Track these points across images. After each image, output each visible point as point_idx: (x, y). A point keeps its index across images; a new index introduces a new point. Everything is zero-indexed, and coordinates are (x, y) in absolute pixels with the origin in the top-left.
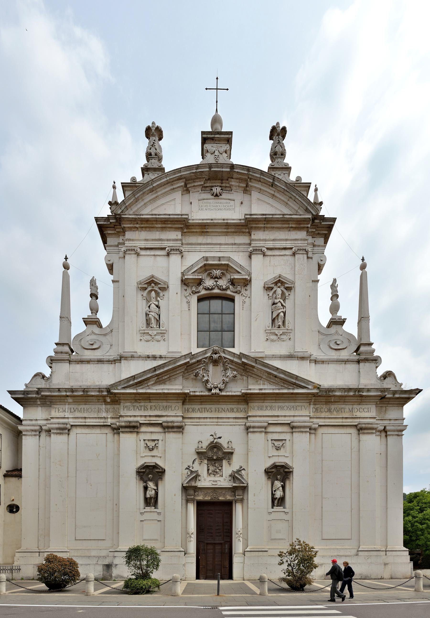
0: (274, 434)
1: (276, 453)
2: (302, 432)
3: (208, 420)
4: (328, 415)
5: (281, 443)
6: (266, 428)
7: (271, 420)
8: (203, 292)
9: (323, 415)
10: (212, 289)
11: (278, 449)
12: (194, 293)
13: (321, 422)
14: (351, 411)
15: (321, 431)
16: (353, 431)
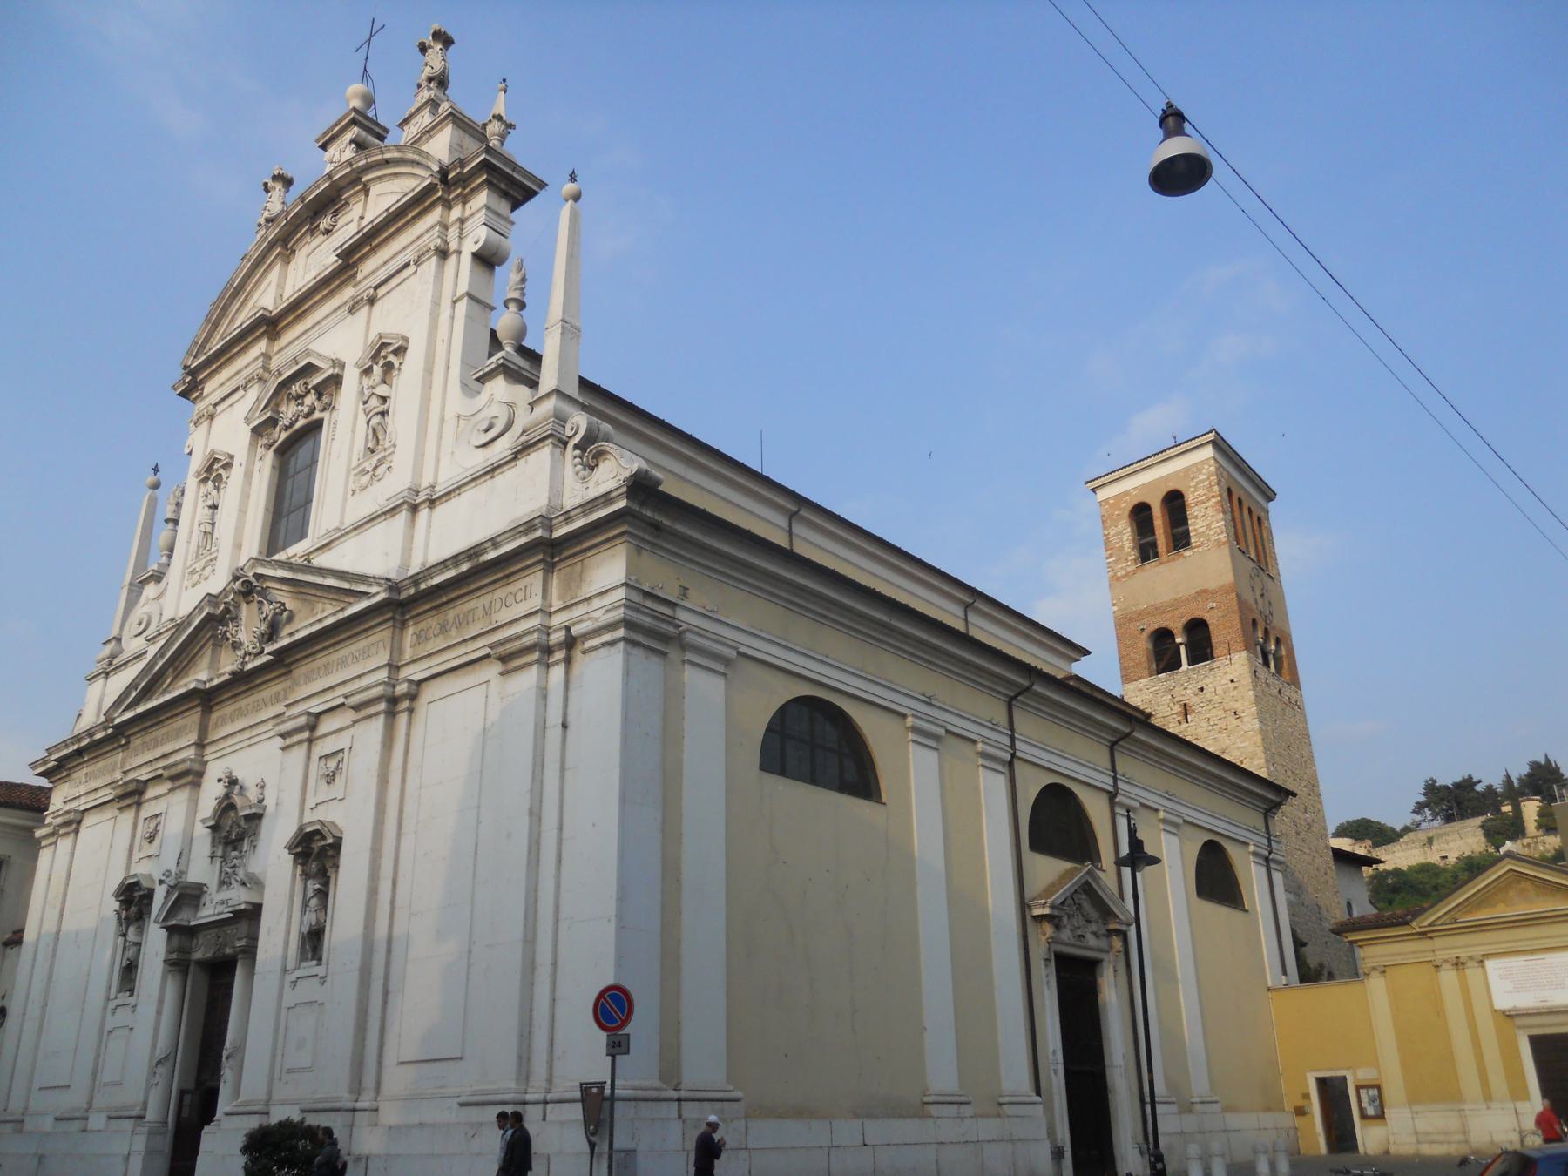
0: (328, 739)
1: (324, 792)
2: (370, 717)
3: (239, 738)
4: (440, 643)
5: (332, 764)
6: (312, 728)
7: (315, 706)
8: (284, 435)
9: (431, 647)
10: (292, 424)
11: (330, 778)
12: (268, 447)
13: (415, 672)
14: (488, 613)
15: (429, 693)
16: (492, 670)
